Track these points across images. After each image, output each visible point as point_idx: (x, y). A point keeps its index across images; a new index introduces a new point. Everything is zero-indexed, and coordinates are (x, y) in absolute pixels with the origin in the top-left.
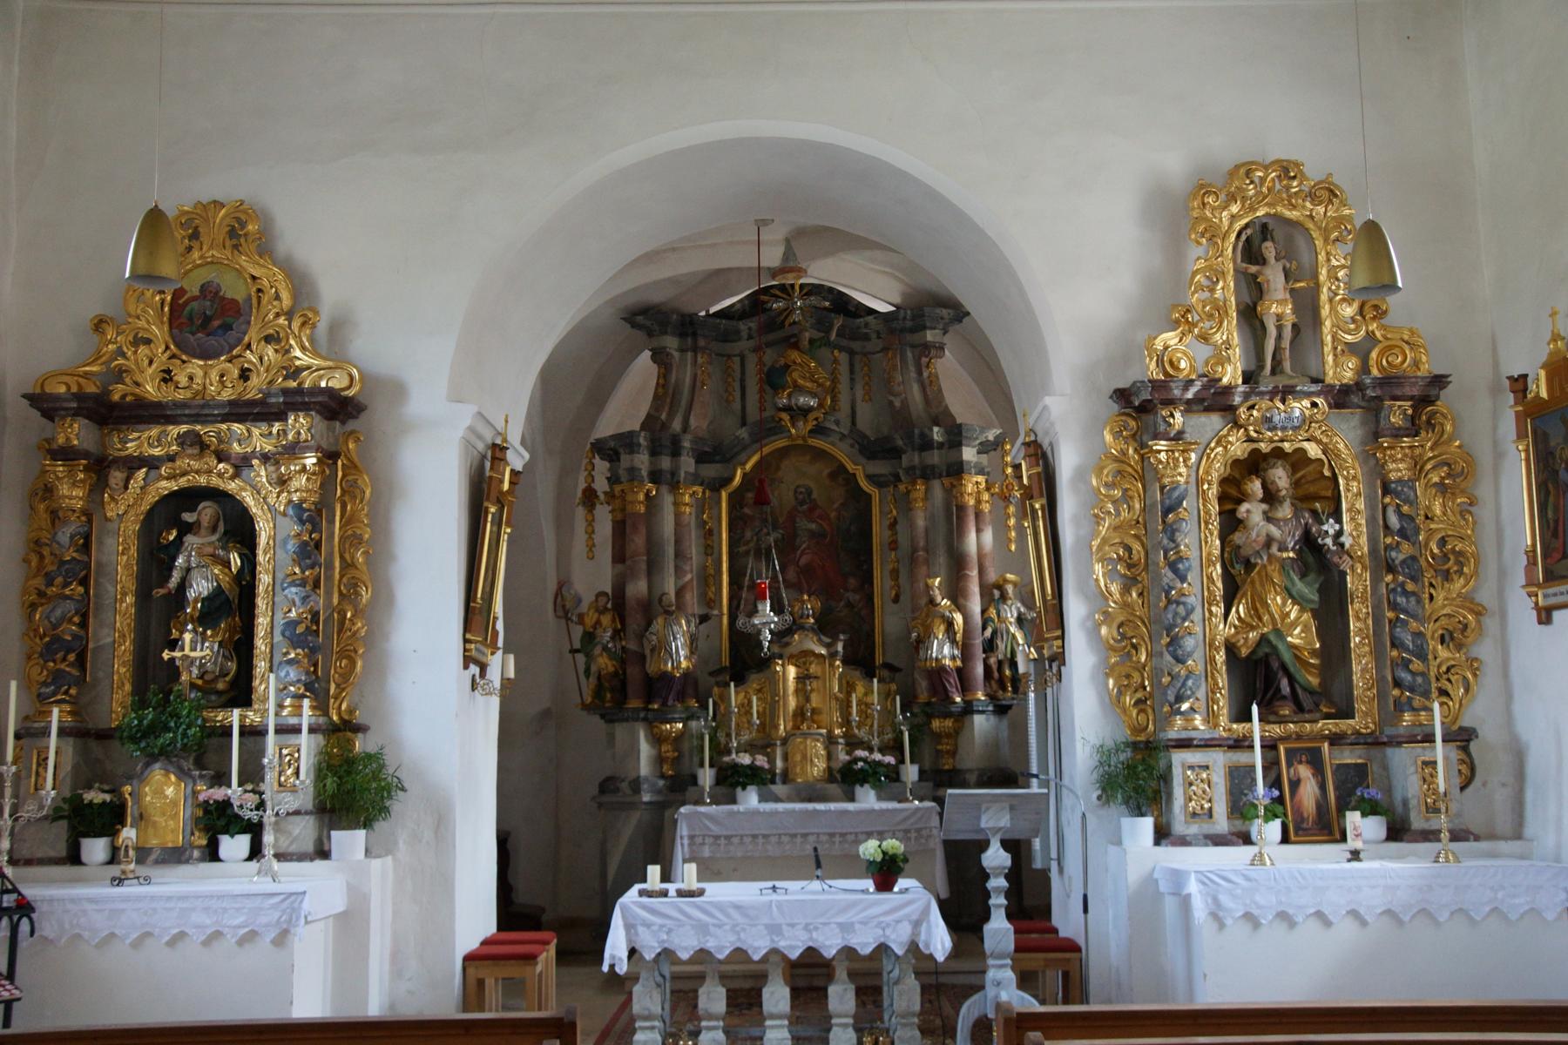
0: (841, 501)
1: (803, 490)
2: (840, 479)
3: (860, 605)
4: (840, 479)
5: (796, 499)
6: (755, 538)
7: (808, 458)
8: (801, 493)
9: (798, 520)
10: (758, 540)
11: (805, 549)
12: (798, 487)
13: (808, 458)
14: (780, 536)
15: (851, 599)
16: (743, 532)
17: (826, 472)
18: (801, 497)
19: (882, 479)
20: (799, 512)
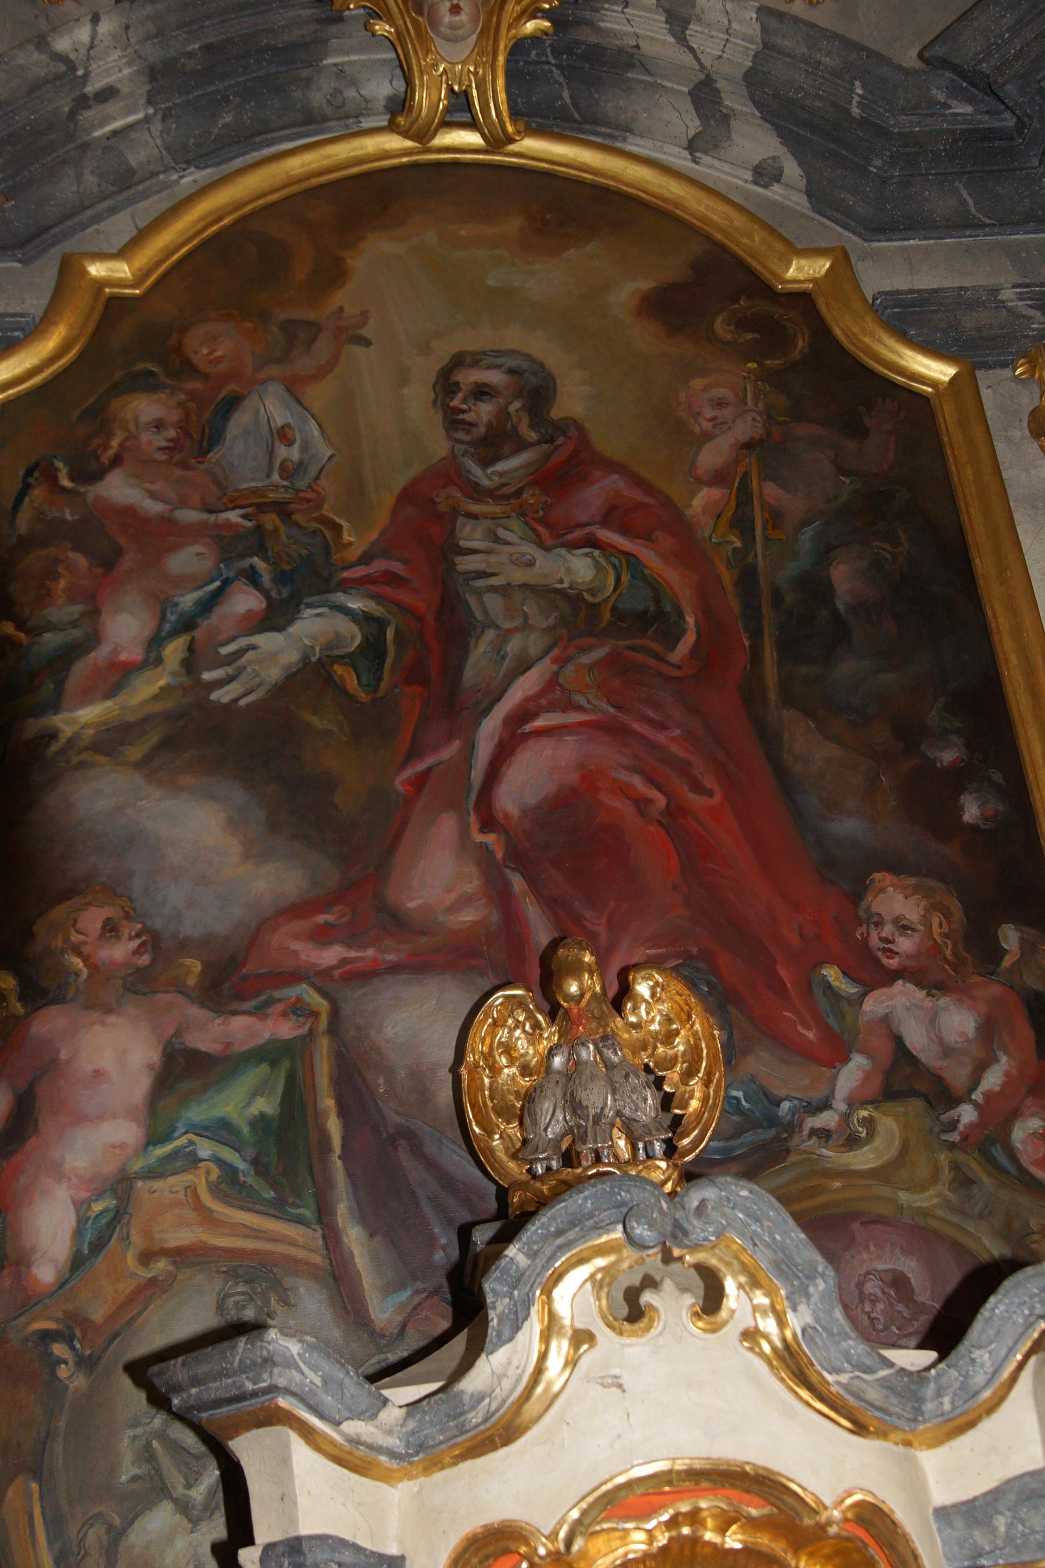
0: (746, 428)
1: (495, 377)
2: (720, 325)
3: (993, 1079)
4: (720, 325)
5: (453, 421)
6: (174, 651)
7: (513, 225)
8: (482, 392)
9: (470, 535)
10: (190, 664)
11: (523, 714)
12: (458, 361)
13: (513, 225)
14: (353, 636)
15: (916, 1038)
16: (94, 613)
17: (645, 285)
18: (484, 411)
19: (969, 321)
20: (476, 492)
